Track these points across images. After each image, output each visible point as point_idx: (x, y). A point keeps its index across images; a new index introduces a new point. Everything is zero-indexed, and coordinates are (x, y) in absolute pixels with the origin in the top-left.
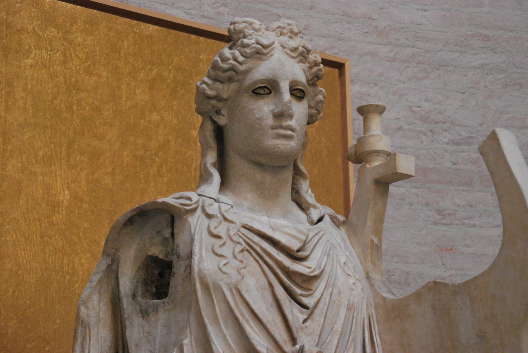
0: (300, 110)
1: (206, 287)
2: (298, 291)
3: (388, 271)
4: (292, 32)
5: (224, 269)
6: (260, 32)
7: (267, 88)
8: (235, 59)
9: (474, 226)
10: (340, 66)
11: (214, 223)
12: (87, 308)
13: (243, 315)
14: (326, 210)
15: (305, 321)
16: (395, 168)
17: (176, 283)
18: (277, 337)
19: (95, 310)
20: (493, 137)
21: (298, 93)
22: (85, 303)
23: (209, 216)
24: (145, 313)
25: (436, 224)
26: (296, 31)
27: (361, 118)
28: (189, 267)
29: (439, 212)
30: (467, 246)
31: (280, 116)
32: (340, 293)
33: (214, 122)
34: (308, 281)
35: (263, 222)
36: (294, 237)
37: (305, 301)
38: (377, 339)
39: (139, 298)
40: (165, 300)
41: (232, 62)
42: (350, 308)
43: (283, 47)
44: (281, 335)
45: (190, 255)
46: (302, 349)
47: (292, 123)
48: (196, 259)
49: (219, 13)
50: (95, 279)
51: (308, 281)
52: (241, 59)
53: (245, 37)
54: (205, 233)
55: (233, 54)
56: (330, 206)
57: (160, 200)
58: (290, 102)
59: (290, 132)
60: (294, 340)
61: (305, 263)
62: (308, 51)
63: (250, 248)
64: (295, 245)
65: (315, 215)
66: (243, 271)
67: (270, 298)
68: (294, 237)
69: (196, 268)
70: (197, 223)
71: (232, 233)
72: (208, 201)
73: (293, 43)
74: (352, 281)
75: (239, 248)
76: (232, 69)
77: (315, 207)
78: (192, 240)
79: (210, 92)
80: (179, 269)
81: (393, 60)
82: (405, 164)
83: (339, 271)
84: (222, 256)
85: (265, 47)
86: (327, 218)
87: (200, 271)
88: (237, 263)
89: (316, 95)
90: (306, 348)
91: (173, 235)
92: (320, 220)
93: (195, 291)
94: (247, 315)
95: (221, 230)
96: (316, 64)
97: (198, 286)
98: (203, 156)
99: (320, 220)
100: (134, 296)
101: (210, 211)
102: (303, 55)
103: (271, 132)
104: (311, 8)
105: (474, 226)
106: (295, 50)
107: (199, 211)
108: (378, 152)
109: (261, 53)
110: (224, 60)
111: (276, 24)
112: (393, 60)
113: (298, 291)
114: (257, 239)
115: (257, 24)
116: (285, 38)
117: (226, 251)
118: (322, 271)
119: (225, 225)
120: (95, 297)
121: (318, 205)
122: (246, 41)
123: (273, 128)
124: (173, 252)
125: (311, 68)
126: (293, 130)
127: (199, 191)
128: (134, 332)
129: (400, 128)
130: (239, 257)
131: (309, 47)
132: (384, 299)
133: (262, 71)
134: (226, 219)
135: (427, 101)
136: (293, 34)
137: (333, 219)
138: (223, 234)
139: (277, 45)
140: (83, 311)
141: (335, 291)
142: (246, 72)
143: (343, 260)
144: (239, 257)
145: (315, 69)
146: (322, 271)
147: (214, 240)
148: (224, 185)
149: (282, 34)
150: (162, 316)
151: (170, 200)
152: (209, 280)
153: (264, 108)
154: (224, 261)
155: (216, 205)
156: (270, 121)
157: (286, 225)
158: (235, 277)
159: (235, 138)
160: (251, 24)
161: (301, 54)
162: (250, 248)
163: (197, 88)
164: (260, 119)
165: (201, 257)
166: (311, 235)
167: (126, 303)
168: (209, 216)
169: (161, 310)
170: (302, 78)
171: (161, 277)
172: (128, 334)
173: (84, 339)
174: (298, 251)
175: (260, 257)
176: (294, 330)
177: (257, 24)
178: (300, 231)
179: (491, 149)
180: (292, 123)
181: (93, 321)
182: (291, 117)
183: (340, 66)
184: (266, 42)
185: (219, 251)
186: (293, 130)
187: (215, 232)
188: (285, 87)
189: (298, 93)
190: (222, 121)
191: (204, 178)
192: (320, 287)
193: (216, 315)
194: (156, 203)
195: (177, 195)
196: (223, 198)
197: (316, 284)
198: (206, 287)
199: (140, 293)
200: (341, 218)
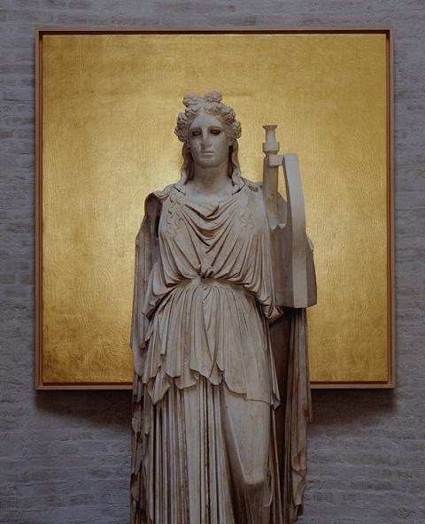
3: (418, 156)
7: (197, 133)
10: (387, 32)
21: (214, 132)
23: (172, 201)
27: (265, 131)
37: (207, 242)
44: (193, 260)
47: (211, 149)
52: (185, 118)
58: (207, 139)
74: (243, 225)
113: (204, 238)
117: (172, 221)
133: (195, 125)
142: (190, 125)
156: (200, 149)
166: (222, 204)
168: (172, 201)
178: (211, 205)
180: (211, 149)
182: (210, 145)
188: (205, 131)
189: (214, 132)
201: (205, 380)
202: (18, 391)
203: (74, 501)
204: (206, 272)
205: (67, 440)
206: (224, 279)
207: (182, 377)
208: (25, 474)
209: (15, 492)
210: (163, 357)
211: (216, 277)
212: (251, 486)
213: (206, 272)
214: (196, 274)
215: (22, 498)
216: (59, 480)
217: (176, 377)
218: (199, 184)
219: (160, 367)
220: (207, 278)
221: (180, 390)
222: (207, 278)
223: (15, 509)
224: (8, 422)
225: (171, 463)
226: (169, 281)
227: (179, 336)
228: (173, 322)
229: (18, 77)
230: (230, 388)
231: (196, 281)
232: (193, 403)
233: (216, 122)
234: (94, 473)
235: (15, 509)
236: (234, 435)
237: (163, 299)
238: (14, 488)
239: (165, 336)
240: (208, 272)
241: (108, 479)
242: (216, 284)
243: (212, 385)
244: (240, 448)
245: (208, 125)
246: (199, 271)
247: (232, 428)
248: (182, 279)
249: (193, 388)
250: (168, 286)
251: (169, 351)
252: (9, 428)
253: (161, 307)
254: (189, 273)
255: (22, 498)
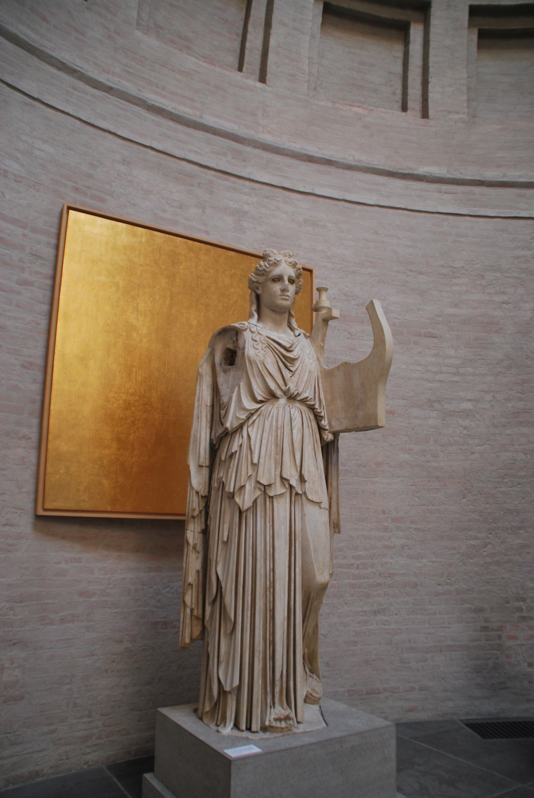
0: (292, 288)
1: (250, 361)
2: (289, 364)
4: (290, 255)
5: (258, 354)
6: (276, 255)
7: (279, 279)
8: (265, 266)
9: (363, 340)
10: (311, 271)
11: (254, 335)
12: (202, 368)
13: (265, 374)
14: (302, 331)
15: (291, 377)
16: (331, 314)
17: (238, 360)
18: (279, 383)
19: (205, 370)
20: (372, 303)
22: (201, 366)
23: (252, 332)
24: (225, 371)
25: (348, 338)
26: (291, 254)
28: (243, 353)
29: (350, 334)
30: (360, 348)
31: (284, 290)
32: (306, 366)
33: (256, 292)
34: (292, 360)
35: (275, 335)
36: (288, 342)
37: (291, 369)
38: (321, 385)
39: (223, 365)
40: (233, 366)
41: (264, 267)
42: (310, 372)
43: (286, 261)
44: (281, 382)
45: (244, 348)
46: (289, 388)
47: (289, 294)
48: (246, 350)
49: (261, 247)
50: (205, 357)
51: (292, 360)
52: (268, 266)
53: (270, 257)
54: (250, 339)
55: (264, 264)
56: (304, 329)
57: (232, 325)
59: (287, 298)
60: (286, 385)
61: (292, 353)
62: (296, 264)
63: (269, 346)
64: (288, 345)
65: (297, 333)
66: (266, 355)
67: (277, 367)
68: (288, 342)
69: (246, 354)
70: (247, 335)
71: (262, 339)
72: (252, 326)
73: (290, 260)
74: (311, 361)
75: (264, 346)
76: (264, 270)
77: (297, 330)
78: (245, 342)
79: (254, 280)
80: (239, 353)
81: (333, 269)
82: (335, 313)
83: (306, 357)
84: (257, 349)
85: (278, 261)
86: (302, 335)
87: (248, 355)
88: (263, 352)
89: (299, 282)
90: (291, 388)
91: (237, 340)
92: (299, 335)
93: (245, 363)
94: (267, 374)
95: (257, 338)
96: (300, 269)
97: (247, 361)
98: (251, 306)
99: (299, 335)
100: (221, 364)
101: (253, 330)
102: (294, 265)
103: (279, 297)
104: (300, 246)
105: (363, 340)
106: (290, 263)
107: (248, 330)
108: (324, 307)
109: (276, 264)
110: (261, 266)
111: (283, 252)
112: (333, 269)
113: (289, 364)
114: (272, 342)
115: (275, 251)
116: (286, 258)
117: (259, 347)
118: (299, 357)
119: (259, 336)
120: (205, 364)
121: (299, 329)
122: (270, 258)
123: (280, 296)
124: (237, 346)
125: (297, 270)
126: (289, 297)
127: (248, 321)
128: (221, 379)
129: (335, 298)
130: (264, 349)
131: (297, 262)
132: (324, 369)
133: (277, 271)
134: (259, 333)
135: (347, 287)
136: (290, 256)
137: (305, 335)
138: (258, 340)
139: (283, 261)
140: (200, 370)
141: (304, 365)
142: (270, 272)
143: (308, 352)
144: (264, 349)
145: (299, 271)
146: (299, 357)
147: (254, 342)
148: (259, 319)
149: (285, 256)
150: (232, 373)
151: (236, 325)
152: (251, 359)
153: (277, 287)
154: (258, 351)
155: (255, 327)
156: (279, 293)
157: (284, 337)
158: (262, 358)
159: (265, 299)
160: (272, 251)
161: (293, 265)
162: (269, 346)
163: (249, 278)
164: (275, 292)
165: (248, 349)
166: (295, 341)
167: (218, 367)
168: (252, 332)
169: (232, 370)
170: (293, 275)
171: (232, 357)
172: (218, 379)
173: (200, 381)
174: (289, 348)
175: (273, 350)
176: (286, 380)
177: (275, 251)
178: (291, 340)
179: (371, 308)
180: (289, 294)
181: (204, 373)
182: (288, 291)
183: (311, 271)
184: (278, 259)
185: (256, 347)
186: (289, 297)
187: (254, 339)
188: (286, 278)
190: (259, 292)
191: (251, 316)
192: (298, 363)
193: (254, 373)
194: (230, 326)
195: (239, 323)
196: (258, 325)
197: (296, 362)
198: (250, 361)
199: (223, 363)
200: (308, 335)
201: (291, 486)
202: (20, 516)
203: (63, 620)
204: (293, 393)
205: (60, 563)
206: (303, 401)
207: (273, 486)
208: (22, 595)
209: (11, 613)
210: (255, 466)
211: (299, 398)
212: (322, 584)
213: (293, 393)
214: (282, 394)
215: (17, 618)
216: (50, 601)
217: (270, 485)
218: (270, 324)
219: (251, 475)
220: (292, 398)
221: (270, 497)
222: (292, 398)
223: (10, 629)
224: (10, 545)
225: (258, 566)
226: (259, 398)
227: (273, 447)
228: (265, 435)
229: (44, 238)
230: (310, 497)
231: (283, 401)
232: (282, 508)
233: (291, 272)
234: (81, 594)
235: (10, 629)
236: (311, 540)
237: (252, 414)
238: (11, 609)
239: (258, 446)
240: (296, 393)
241: (93, 599)
242: (298, 405)
243: (297, 494)
244: (315, 551)
245: (288, 274)
246: (285, 393)
247: (309, 533)
248: (273, 396)
249: (281, 495)
250: (261, 402)
251: (262, 461)
252: (9, 551)
253: (251, 421)
254: (279, 393)
255: (17, 618)
